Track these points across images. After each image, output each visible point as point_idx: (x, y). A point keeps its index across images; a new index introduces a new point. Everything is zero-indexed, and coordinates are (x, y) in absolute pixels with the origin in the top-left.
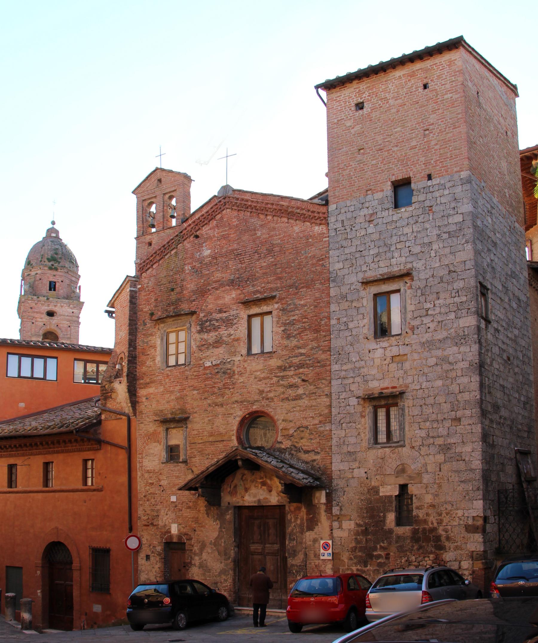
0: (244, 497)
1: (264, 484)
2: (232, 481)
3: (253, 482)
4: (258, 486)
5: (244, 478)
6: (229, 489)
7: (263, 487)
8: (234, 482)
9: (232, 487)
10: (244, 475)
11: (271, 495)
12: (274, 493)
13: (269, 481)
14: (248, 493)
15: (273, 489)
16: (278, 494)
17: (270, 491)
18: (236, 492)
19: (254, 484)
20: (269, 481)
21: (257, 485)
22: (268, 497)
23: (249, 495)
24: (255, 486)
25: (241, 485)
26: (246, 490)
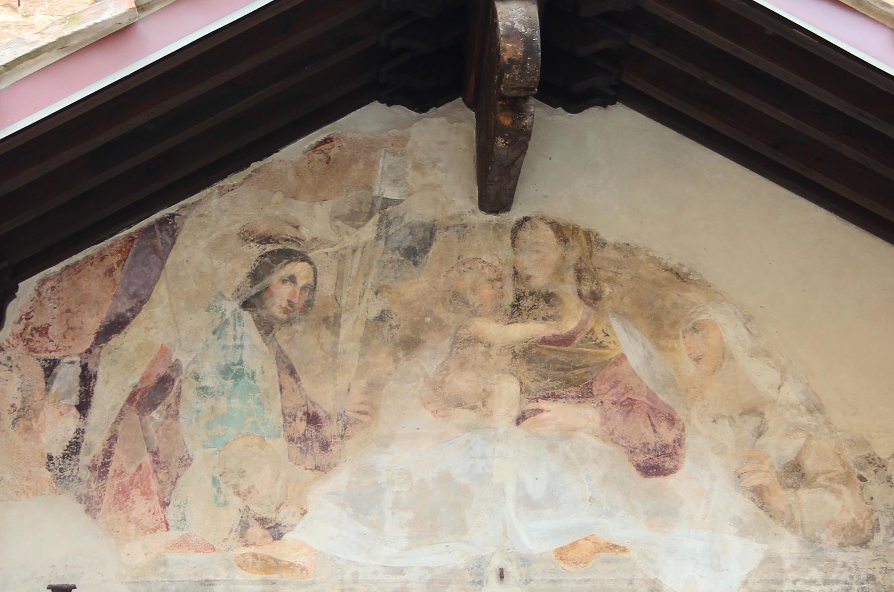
0: (276, 531)
1: (564, 370)
2: (115, 326)
3: (410, 344)
4: (481, 402)
5: (282, 295)
6: (57, 426)
7: (558, 413)
8: (127, 341)
9: (109, 395)
10: (280, 251)
11: (664, 514)
12: (706, 483)
13: (630, 345)
14: (340, 479)
15: (694, 443)
16: (759, 494)
17: (655, 465)
18: (167, 465)
19: (428, 361)
20: (630, 345)
21: (463, 383)
22: (619, 528)
23: (361, 505)
24: (447, 402)
25: (232, 372)
26: (313, 434)
